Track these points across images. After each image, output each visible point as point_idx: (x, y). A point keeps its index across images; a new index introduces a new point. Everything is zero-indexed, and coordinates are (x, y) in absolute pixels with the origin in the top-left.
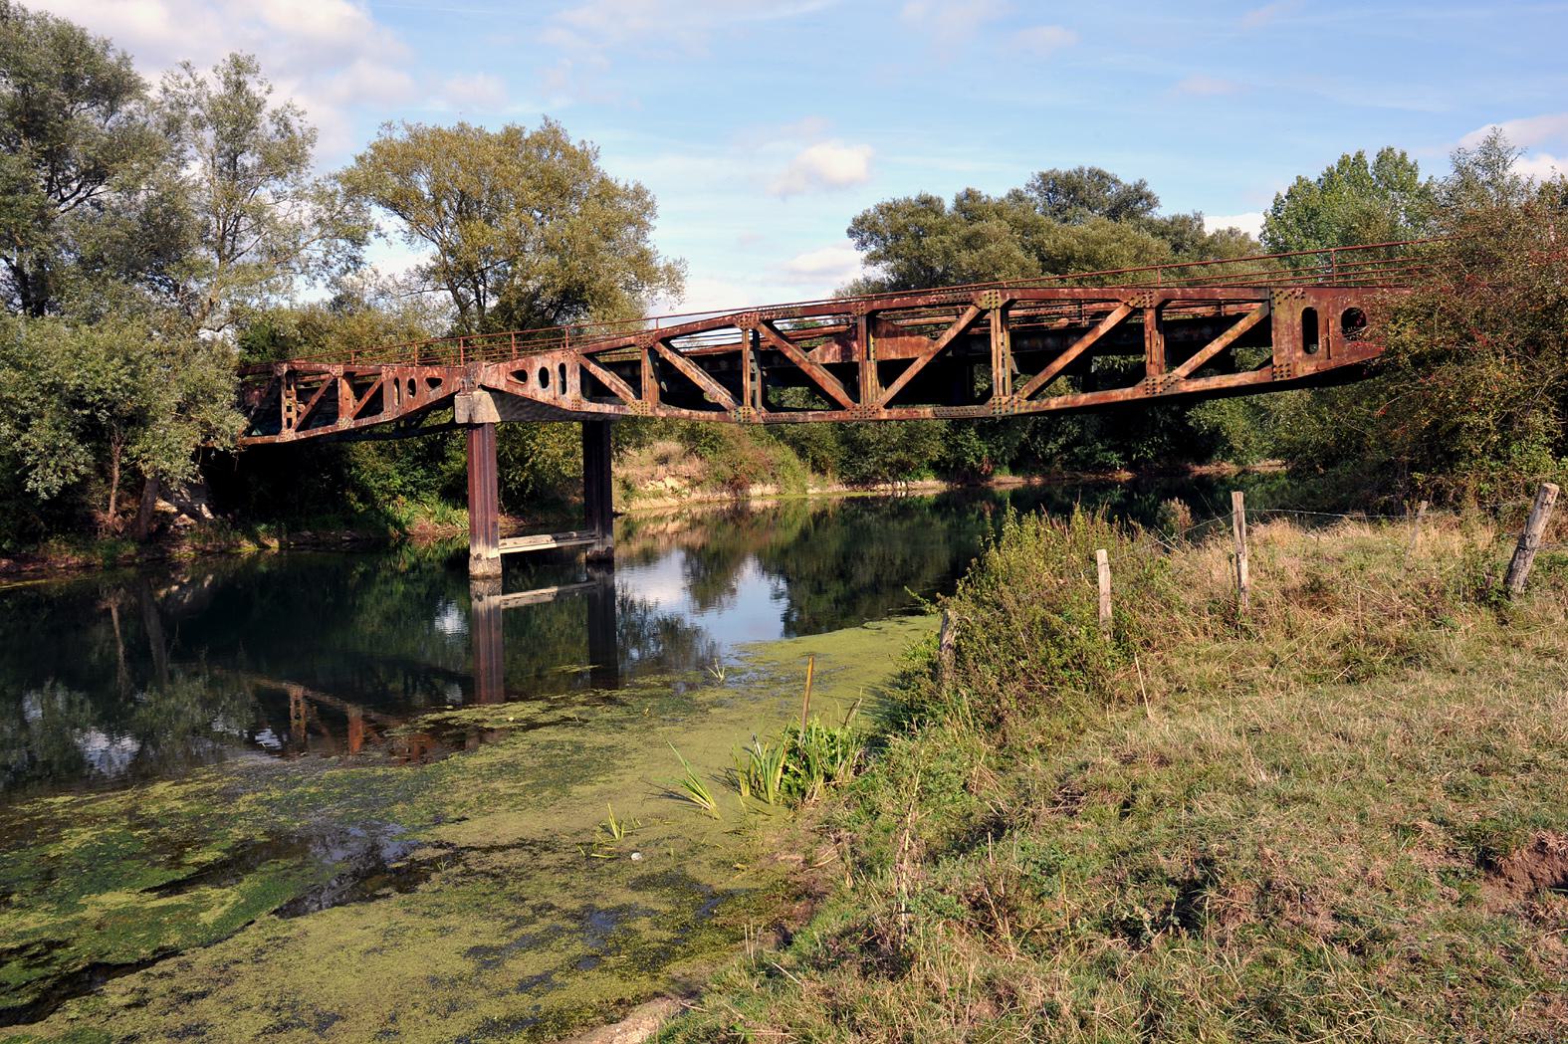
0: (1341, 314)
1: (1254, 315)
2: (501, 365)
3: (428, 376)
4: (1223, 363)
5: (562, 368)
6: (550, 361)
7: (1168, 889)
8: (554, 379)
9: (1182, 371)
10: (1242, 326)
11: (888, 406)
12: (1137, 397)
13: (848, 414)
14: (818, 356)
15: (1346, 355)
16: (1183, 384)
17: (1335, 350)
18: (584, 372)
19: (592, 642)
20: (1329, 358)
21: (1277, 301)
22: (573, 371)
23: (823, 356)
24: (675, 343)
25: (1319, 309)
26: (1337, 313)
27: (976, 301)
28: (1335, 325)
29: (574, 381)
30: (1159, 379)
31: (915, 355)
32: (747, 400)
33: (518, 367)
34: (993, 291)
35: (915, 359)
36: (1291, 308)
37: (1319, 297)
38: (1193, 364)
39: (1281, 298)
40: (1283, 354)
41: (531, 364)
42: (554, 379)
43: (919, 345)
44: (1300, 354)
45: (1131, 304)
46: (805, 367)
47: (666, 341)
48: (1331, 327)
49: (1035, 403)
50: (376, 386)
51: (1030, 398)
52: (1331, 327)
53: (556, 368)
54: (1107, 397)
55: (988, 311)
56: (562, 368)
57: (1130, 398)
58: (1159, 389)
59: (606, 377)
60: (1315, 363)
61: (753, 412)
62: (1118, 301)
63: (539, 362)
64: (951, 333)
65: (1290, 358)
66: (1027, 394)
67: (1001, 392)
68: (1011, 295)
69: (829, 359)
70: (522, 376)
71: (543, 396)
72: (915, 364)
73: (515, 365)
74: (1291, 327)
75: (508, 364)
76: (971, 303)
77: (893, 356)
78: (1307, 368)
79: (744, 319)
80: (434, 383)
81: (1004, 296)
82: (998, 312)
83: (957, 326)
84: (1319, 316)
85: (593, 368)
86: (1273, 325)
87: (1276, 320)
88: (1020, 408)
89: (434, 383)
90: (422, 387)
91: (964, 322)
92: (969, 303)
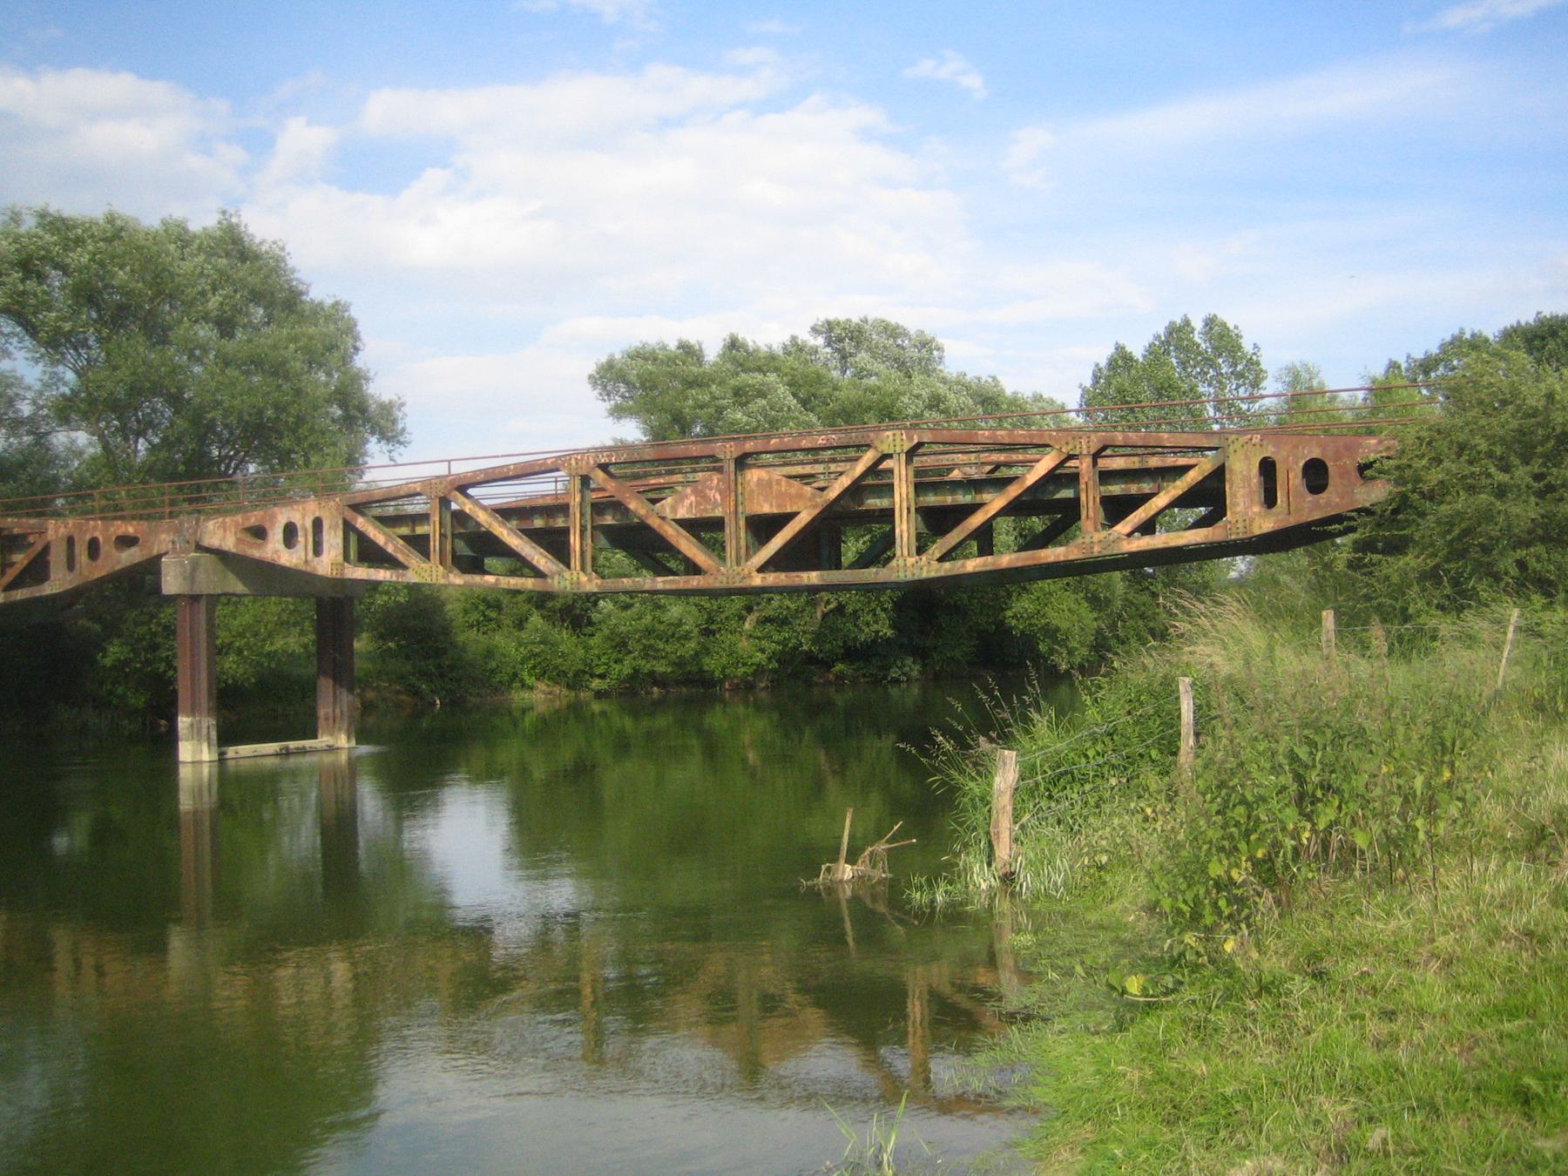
0: (1301, 464)
1: (1202, 467)
2: (228, 520)
3: (120, 532)
4: (1147, 528)
5: (318, 524)
6: (301, 514)
7: (1253, 1007)
8: (304, 539)
9: (1123, 527)
10: (1192, 477)
11: (761, 569)
12: (1071, 557)
13: (711, 580)
14: (668, 510)
15: (1309, 508)
16: (1125, 543)
17: (1298, 506)
18: (348, 527)
19: (1108, 570)
20: (1289, 513)
21: (1231, 449)
22: (333, 527)
23: (674, 509)
24: (471, 491)
25: (1277, 458)
26: (1297, 463)
27: (877, 443)
28: (1296, 477)
29: (333, 541)
30: (1098, 536)
31: (795, 509)
32: (575, 561)
33: (254, 519)
34: (898, 432)
35: (797, 514)
36: (1247, 458)
37: (1276, 446)
38: (1136, 520)
39: (1237, 445)
40: (1238, 509)
41: (273, 518)
42: (304, 539)
43: (800, 496)
44: (1256, 509)
45: (1064, 450)
46: (654, 522)
47: (462, 489)
48: (1291, 477)
49: (947, 565)
50: (39, 547)
51: (941, 560)
52: (1291, 477)
53: (309, 524)
54: (1034, 559)
55: (890, 456)
56: (318, 524)
57: (1062, 559)
58: (1096, 549)
59: (378, 536)
60: (1273, 518)
61: (584, 578)
62: (1048, 446)
63: (283, 516)
64: (845, 481)
65: (1247, 514)
66: (938, 555)
67: (906, 553)
68: (919, 437)
69: (682, 513)
70: (259, 533)
71: (289, 558)
72: (797, 518)
73: (248, 519)
74: (1247, 479)
75: (239, 518)
76: (869, 446)
77: (766, 509)
78: (1265, 524)
79: (573, 462)
80: (126, 542)
81: (910, 438)
82: (903, 457)
83: (850, 474)
84: (1277, 466)
85: (361, 523)
86: (1227, 476)
87: (1231, 471)
88: (928, 572)
89: (126, 542)
90: (106, 548)
91: (860, 468)
92: (863, 447)
